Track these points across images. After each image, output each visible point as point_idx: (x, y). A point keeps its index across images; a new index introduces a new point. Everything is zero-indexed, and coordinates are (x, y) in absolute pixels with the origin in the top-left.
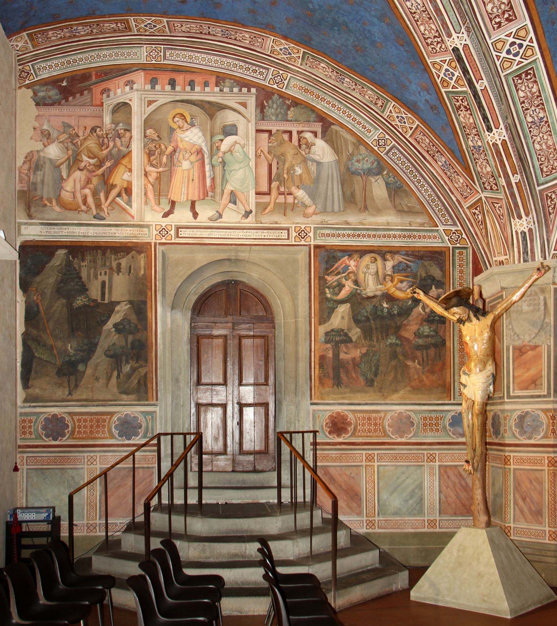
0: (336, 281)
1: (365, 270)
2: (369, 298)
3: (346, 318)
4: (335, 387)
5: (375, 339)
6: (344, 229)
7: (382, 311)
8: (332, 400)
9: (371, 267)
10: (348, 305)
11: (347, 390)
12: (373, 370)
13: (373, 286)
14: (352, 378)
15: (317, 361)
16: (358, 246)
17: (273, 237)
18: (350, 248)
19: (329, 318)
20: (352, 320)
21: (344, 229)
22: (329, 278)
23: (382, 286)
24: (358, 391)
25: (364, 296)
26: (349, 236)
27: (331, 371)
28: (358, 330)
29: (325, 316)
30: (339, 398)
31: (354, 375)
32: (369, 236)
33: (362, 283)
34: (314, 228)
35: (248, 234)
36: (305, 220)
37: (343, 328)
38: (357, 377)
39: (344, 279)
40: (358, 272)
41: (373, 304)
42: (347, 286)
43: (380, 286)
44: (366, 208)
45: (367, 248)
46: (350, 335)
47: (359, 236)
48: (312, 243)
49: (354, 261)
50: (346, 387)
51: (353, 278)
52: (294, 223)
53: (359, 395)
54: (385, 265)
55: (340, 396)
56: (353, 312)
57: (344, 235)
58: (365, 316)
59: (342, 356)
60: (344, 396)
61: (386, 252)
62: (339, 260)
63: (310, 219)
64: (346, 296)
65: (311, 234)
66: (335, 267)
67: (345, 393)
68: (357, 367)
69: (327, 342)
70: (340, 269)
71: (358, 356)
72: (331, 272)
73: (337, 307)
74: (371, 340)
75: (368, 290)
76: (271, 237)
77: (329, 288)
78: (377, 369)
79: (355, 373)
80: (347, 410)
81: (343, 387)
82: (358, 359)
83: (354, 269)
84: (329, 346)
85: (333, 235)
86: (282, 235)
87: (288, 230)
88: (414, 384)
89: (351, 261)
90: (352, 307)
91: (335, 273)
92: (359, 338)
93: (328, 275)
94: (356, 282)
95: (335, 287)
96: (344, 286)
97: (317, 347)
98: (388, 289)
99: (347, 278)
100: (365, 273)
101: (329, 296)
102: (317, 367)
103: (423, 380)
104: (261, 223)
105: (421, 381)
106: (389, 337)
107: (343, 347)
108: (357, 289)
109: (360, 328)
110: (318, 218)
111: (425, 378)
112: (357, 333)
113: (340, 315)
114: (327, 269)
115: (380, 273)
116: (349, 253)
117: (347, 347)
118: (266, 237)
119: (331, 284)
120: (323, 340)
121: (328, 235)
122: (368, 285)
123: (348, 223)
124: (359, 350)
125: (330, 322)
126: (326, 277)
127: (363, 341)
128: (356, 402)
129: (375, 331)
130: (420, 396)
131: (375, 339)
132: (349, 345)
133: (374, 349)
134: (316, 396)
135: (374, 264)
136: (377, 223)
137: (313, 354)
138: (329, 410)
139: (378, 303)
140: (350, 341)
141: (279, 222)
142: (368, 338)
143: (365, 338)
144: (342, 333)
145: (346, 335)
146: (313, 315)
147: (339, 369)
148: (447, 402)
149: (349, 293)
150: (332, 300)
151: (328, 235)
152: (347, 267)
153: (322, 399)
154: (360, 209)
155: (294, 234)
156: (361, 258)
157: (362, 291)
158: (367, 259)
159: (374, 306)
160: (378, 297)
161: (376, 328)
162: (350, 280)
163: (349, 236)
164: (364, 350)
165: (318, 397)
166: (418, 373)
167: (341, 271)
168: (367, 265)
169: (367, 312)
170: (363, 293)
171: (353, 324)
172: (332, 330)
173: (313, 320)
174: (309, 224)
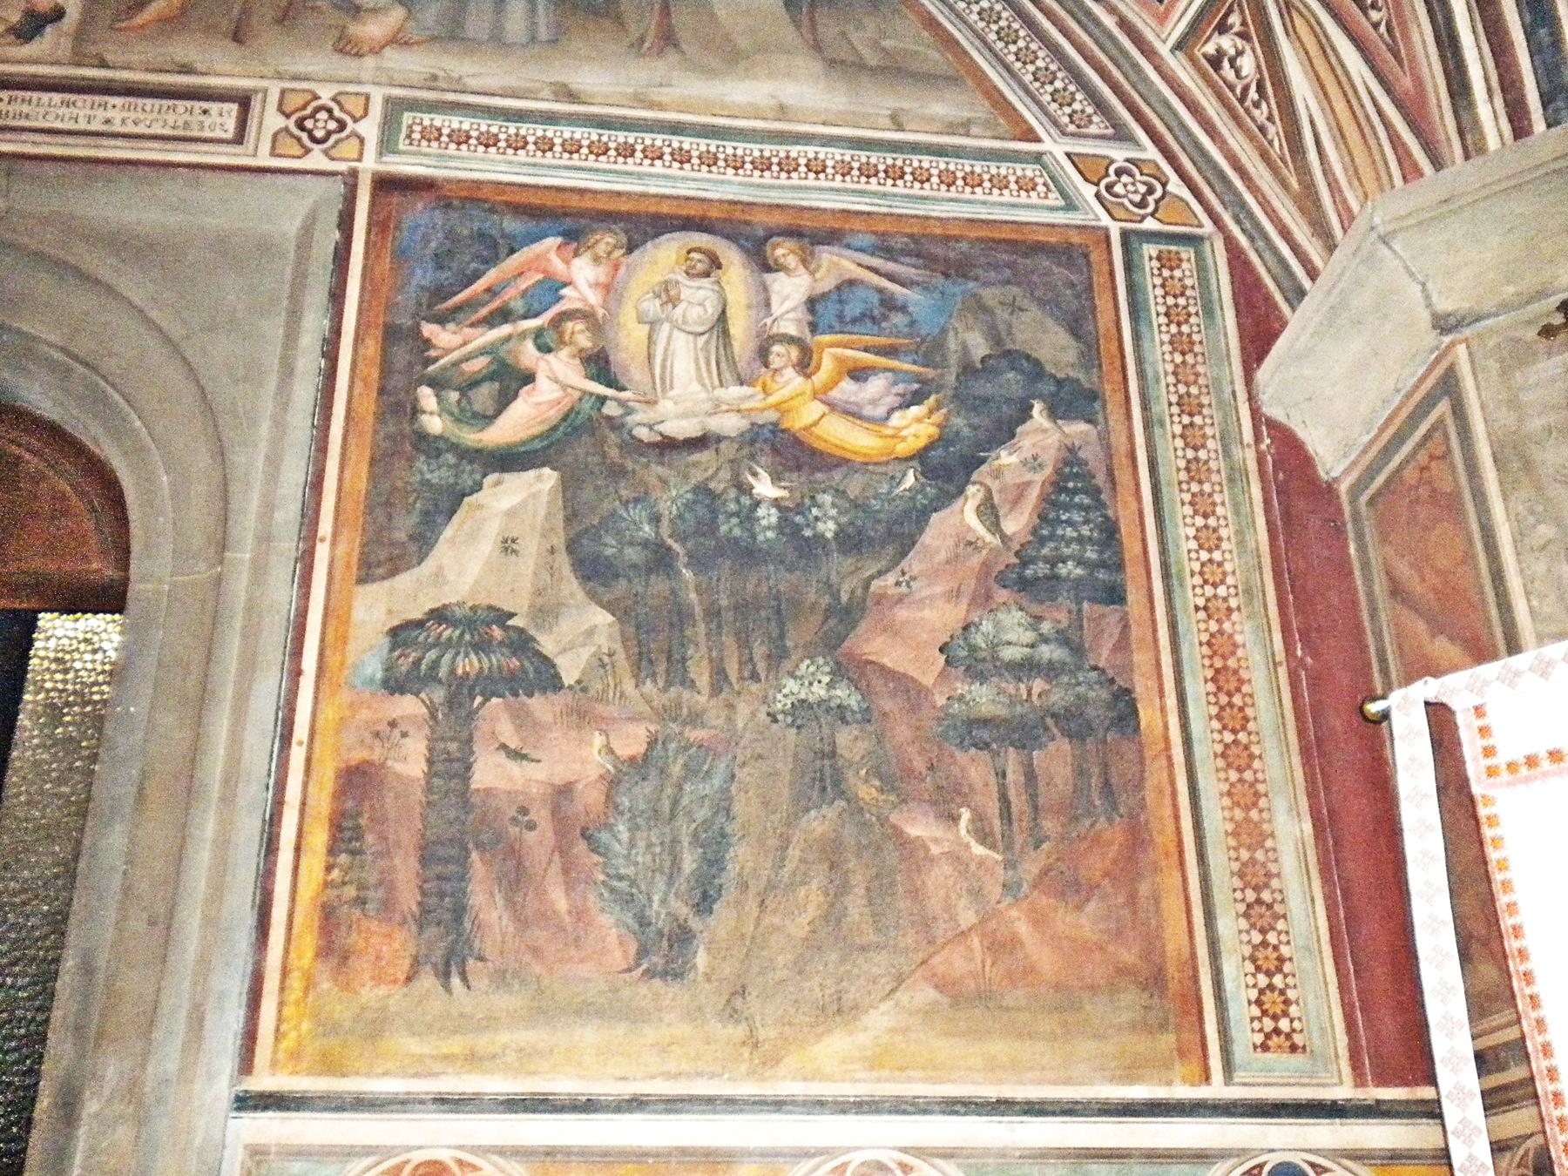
0: (482, 352)
1: (653, 307)
2: (668, 446)
3: (531, 548)
4: (428, 982)
5: (701, 674)
6: (550, 118)
7: (748, 517)
8: (404, 1074)
9: (685, 293)
10: (547, 479)
11: (505, 1002)
12: (689, 862)
13: (696, 387)
14: (546, 916)
15: (322, 802)
16: (619, 194)
17: (157, 129)
18: (574, 202)
19: (424, 541)
20: (563, 561)
21: (550, 118)
22: (441, 336)
23: (745, 390)
24: (584, 1011)
25: (643, 433)
26: (572, 148)
27: (406, 871)
28: (602, 618)
29: (401, 536)
30: (448, 1058)
31: (559, 899)
32: (683, 158)
33: (636, 373)
34: (388, 100)
35: (25, 109)
36: (348, 67)
37: (507, 607)
38: (579, 914)
39: (529, 346)
40: (612, 314)
41: (697, 477)
42: (542, 381)
43: (735, 391)
44: (668, 39)
45: (665, 208)
46: (547, 644)
47: (627, 151)
48: (370, 164)
49: (597, 260)
50: (501, 978)
51: (584, 341)
52: (279, 76)
53: (589, 1035)
54: (765, 288)
55: (455, 1045)
56: (571, 517)
57: (546, 146)
58: (645, 544)
59: (489, 772)
60: (483, 1042)
61: (771, 234)
62: (512, 251)
63: (370, 62)
64: (536, 430)
65: (369, 129)
66: (480, 285)
67: (491, 1022)
68: (582, 846)
69: (394, 685)
70: (511, 297)
71: (593, 773)
72: (458, 308)
73: (477, 487)
74: (678, 673)
75: (666, 406)
76: (141, 129)
77: (437, 384)
78: (714, 862)
79: (569, 888)
80: (501, 1151)
81: (480, 982)
82: (591, 797)
83: (594, 298)
84: (408, 706)
85: (489, 141)
86: (207, 121)
87: (244, 101)
88: (957, 962)
89: (577, 262)
90: (570, 485)
91: (484, 311)
92: (601, 664)
93: (441, 320)
94: (599, 365)
95: (474, 383)
96: (529, 378)
97: (329, 713)
98: (777, 407)
99: (550, 337)
100: (653, 324)
101: (434, 424)
102: (319, 838)
103: (1014, 942)
104: (103, 64)
105: (1002, 946)
106: (787, 665)
107: (496, 717)
108: (602, 400)
109: (609, 607)
110: (412, 64)
111: (1023, 928)
112: (590, 633)
113: (492, 531)
114: (440, 293)
115: (739, 327)
116: (568, 223)
117: (521, 719)
118: (117, 128)
119: (456, 364)
120: (374, 668)
121: (461, 139)
122: (667, 383)
123: (572, 96)
124: (598, 740)
125: (429, 565)
126: (428, 329)
127: (628, 685)
128: (563, 1085)
129: (702, 628)
130: (998, 1047)
131: (701, 674)
132: (539, 705)
133: (695, 734)
134: (288, 1044)
135: (705, 282)
136: (723, 106)
137: (297, 755)
138: (368, 1151)
139: (725, 474)
140: (548, 678)
141: (199, 66)
142: (661, 668)
143: (642, 663)
144: (497, 632)
145: (522, 643)
146: (326, 526)
147: (463, 861)
148: (1182, 1092)
149: (554, 415)
150: (454, 447)
151: (461, 139)
152: (553, 287)
153: (329, 1065)
154: (642, 40)
155: (274, 122)
156: (631, 248)
157: (629, 411)
158: (666, 253)
159: (702, 490)
160: (723, 446)
161: (713, 613)
162: (564, 353)
163: (572, 148)
164: (632, 741)
165: (295, 1056)
166: (976, 894)
167: (518, 306)
168: (666, 286)
169: (656, 519)
170: (637, 417)
171: (571, 586)
172: (439, 615)
173: (322, 553)
174: (360, 83)
